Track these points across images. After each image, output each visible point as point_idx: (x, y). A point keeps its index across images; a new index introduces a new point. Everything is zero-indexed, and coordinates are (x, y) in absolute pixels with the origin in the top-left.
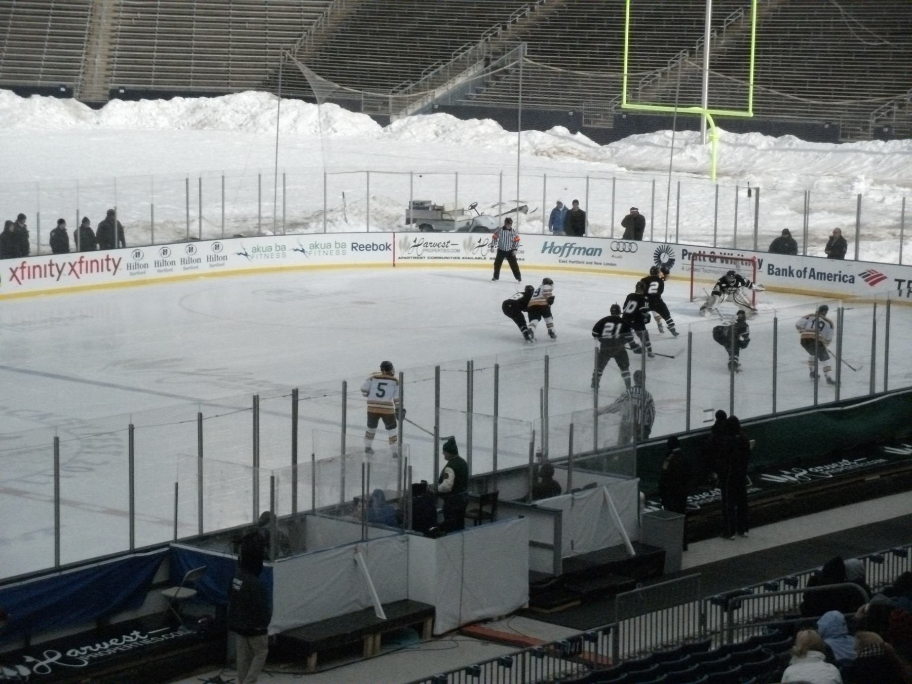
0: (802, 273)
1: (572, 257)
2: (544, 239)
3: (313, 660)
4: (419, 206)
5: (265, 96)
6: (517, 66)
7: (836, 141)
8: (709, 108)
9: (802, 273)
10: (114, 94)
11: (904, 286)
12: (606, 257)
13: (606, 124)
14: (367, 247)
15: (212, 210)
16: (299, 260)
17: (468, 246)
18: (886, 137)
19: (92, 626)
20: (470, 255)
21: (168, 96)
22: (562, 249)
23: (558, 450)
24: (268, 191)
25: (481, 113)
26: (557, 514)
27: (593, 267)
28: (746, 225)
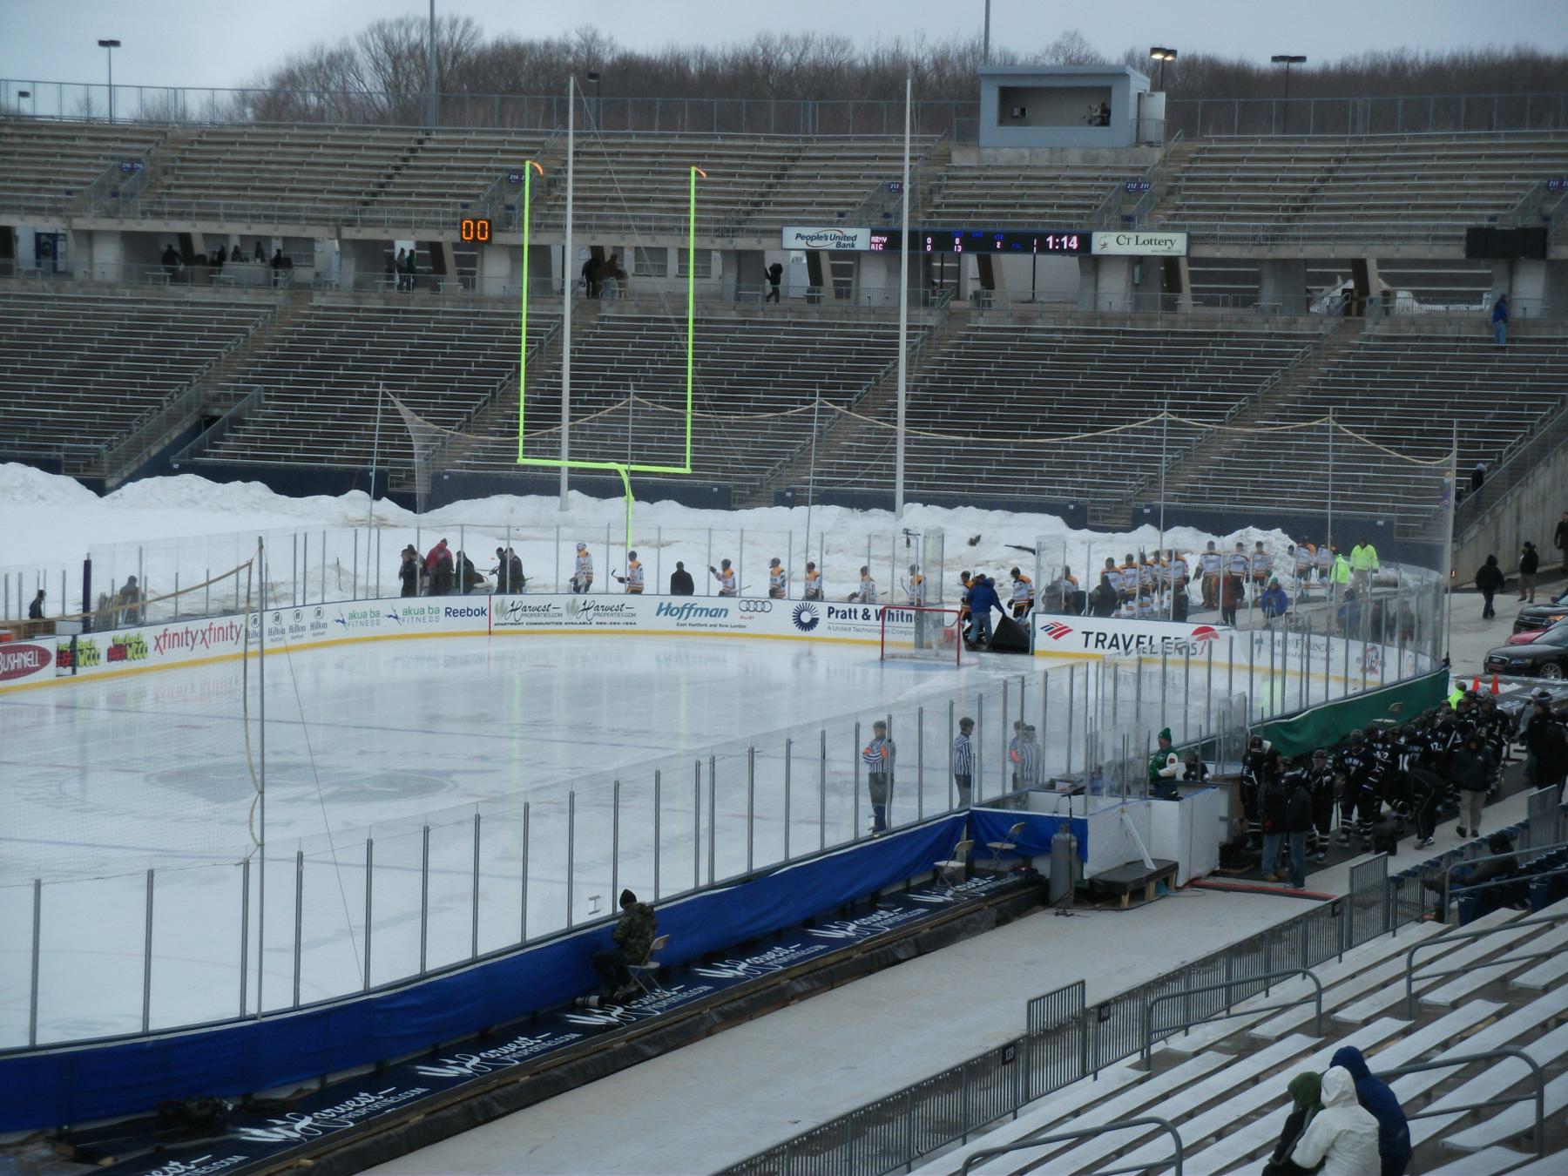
1: (692, 619)
2: (659, 600)
3: (1125, 899)
6: (627, 404)
7: (728, 508)
8: (558, 469)
11: (1092, 638)
12: (734, 617)
14: (462, 612)
16: (391, 627)
18: (791, 503)
19: (929, 877)
20: (574, 620)
22: (680, 611)
25: (246, 475)
27: (718, 630)
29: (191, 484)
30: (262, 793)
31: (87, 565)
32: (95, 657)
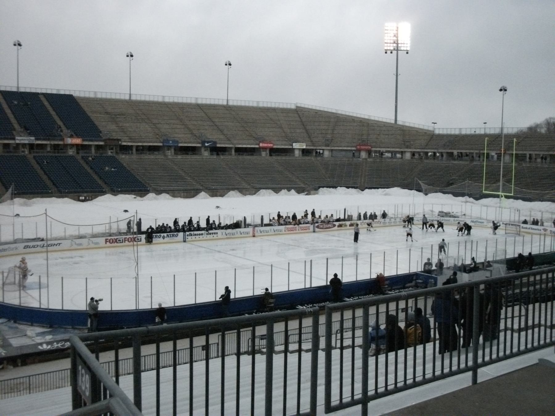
0: (529, 228)
4: (440, 212)
5: (399, 188)
9: (529, 228)
10: (367, 188)
12: (485, 224)
13: (478, 196)
15: (400, 211)
17: (454, 220)
18: (542, 201)
21: (378, 188)
23: (490, 259)
24: (411, 208)
26: (491, 271)
28: (517, 219)
29: (440, 194)
30: (137, 264)
31: (345, 209)
32: (346, 226)
